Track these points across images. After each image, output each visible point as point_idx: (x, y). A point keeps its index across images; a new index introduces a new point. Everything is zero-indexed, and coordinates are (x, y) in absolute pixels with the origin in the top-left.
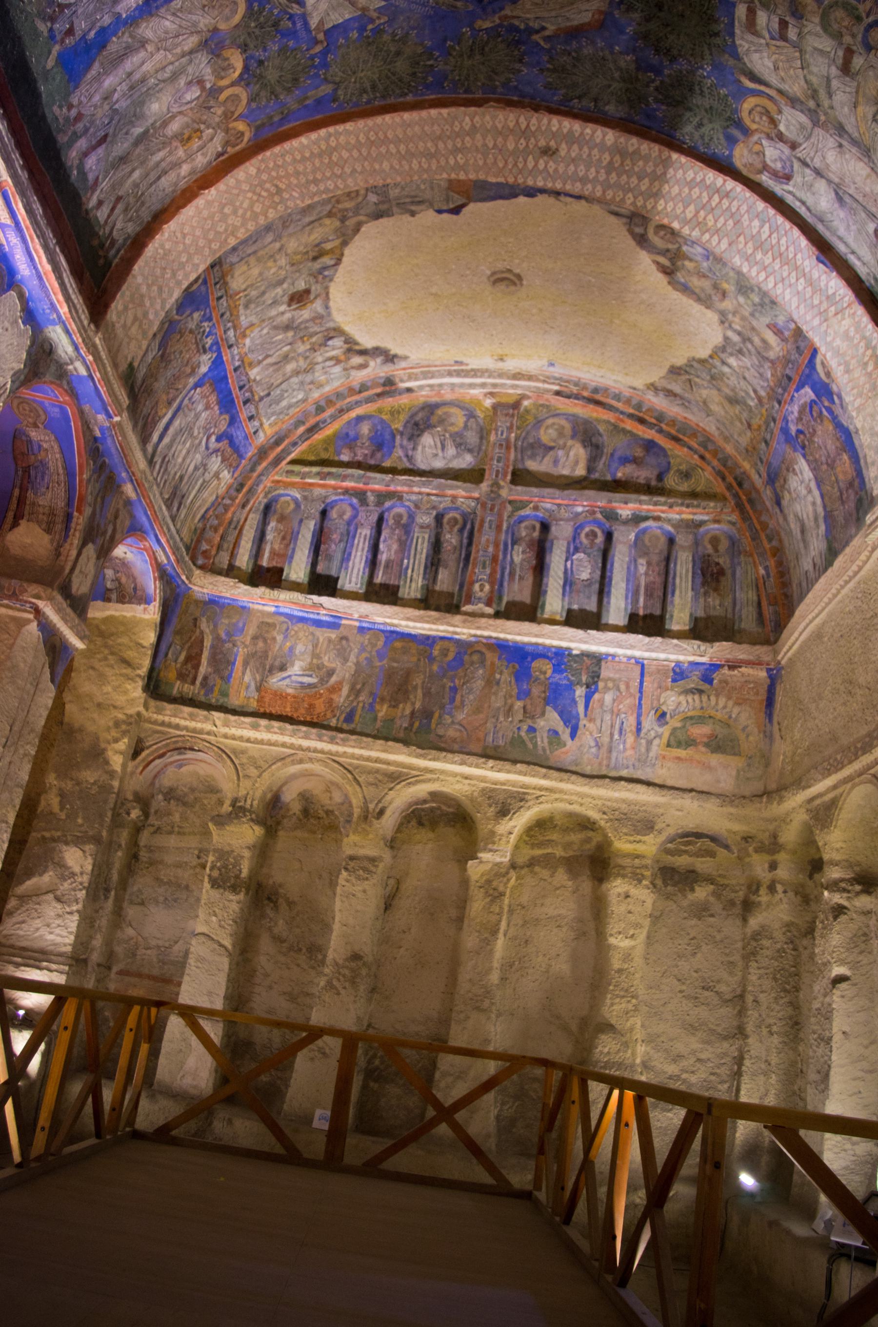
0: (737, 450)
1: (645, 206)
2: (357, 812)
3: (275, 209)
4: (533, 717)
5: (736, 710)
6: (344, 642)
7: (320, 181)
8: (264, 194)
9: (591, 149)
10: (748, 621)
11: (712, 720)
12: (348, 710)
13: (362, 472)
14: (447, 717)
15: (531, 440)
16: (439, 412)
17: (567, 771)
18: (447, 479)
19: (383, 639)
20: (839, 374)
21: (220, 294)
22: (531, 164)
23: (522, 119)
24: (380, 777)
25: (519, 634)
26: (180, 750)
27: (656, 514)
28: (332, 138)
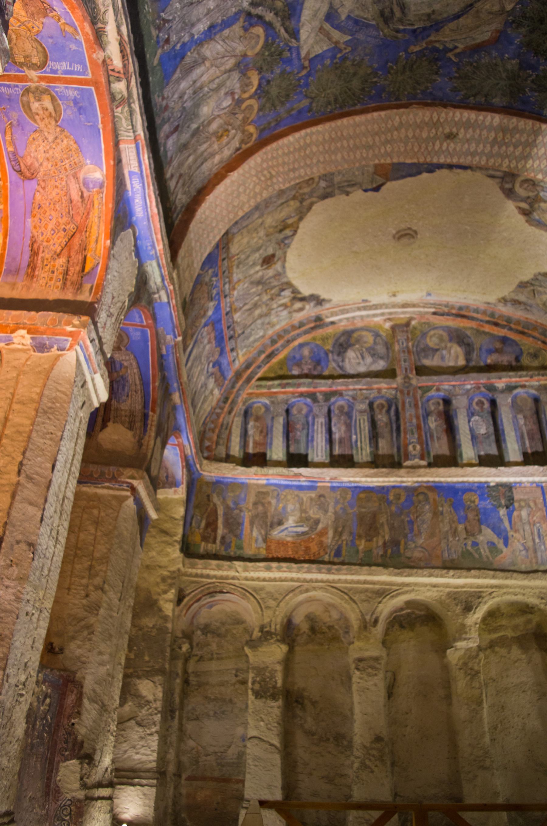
1: (517, 167)
2: (355, 623)
3: (267, 190)
4: (473, 535)
6: (322, 499)
8: (263, 179)
9: (481, 130)
12: (336, 547)
13: (310, 380)
14: (410, 543)
15: (422, 346)
16: (355, 335)
17: (509, 571)
18: (371, 377)
21: (224, 256)
23: (435, 115)
24: (370, 595)
25: (450, 477)
26: (212, 594)
27: (522, 383)
28: (308, 137)
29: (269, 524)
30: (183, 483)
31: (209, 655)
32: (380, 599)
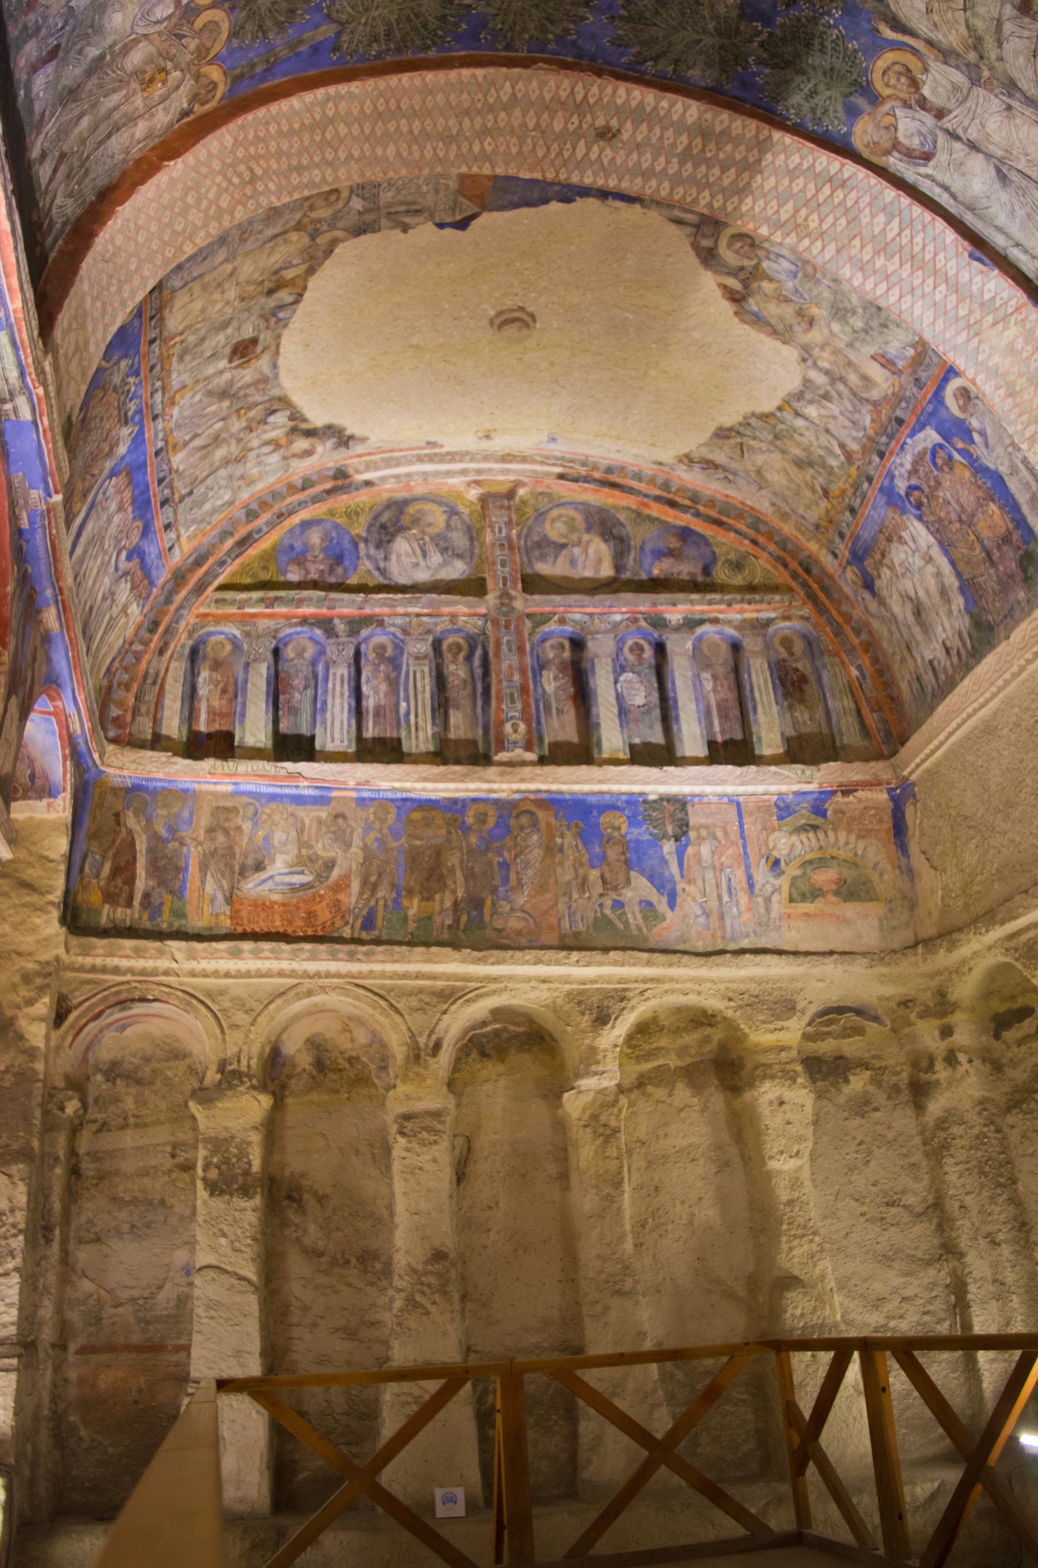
0: (799, 529)
2: (399, 1051)
3: (245, 205)
4: (616, 888)
5: (861, 845)
6: (340, 821)
7: (306, 168)
8: (236, 180)
9: (664, 129)
10: (850, 734)
11: (835, 862)
12: (365, 912)
13: (322, 594)
14: (502, 903)
15: (536, 538)
16: (411, 510)
17: (675, 952)
18: (440, 593)
19: (394, 811)
20: (997, 400)
21: (153, 336)
22: (581, 151)
23: (579, 88)
24: (427, 999)
25: (577, 783)
26: (123, 1004)
27: (712, 615)
28: (331, 105)
29: (237, 868)
30: (64, 790)
31: (120, 1120)
32: (445, 1007)
